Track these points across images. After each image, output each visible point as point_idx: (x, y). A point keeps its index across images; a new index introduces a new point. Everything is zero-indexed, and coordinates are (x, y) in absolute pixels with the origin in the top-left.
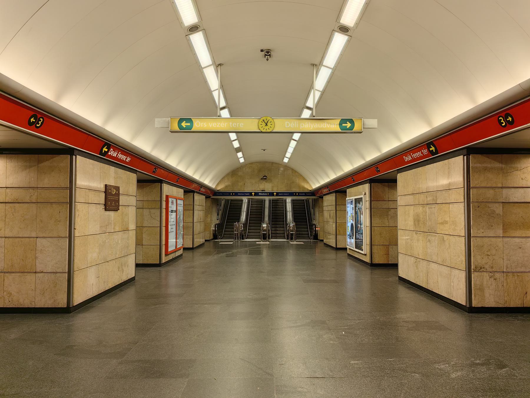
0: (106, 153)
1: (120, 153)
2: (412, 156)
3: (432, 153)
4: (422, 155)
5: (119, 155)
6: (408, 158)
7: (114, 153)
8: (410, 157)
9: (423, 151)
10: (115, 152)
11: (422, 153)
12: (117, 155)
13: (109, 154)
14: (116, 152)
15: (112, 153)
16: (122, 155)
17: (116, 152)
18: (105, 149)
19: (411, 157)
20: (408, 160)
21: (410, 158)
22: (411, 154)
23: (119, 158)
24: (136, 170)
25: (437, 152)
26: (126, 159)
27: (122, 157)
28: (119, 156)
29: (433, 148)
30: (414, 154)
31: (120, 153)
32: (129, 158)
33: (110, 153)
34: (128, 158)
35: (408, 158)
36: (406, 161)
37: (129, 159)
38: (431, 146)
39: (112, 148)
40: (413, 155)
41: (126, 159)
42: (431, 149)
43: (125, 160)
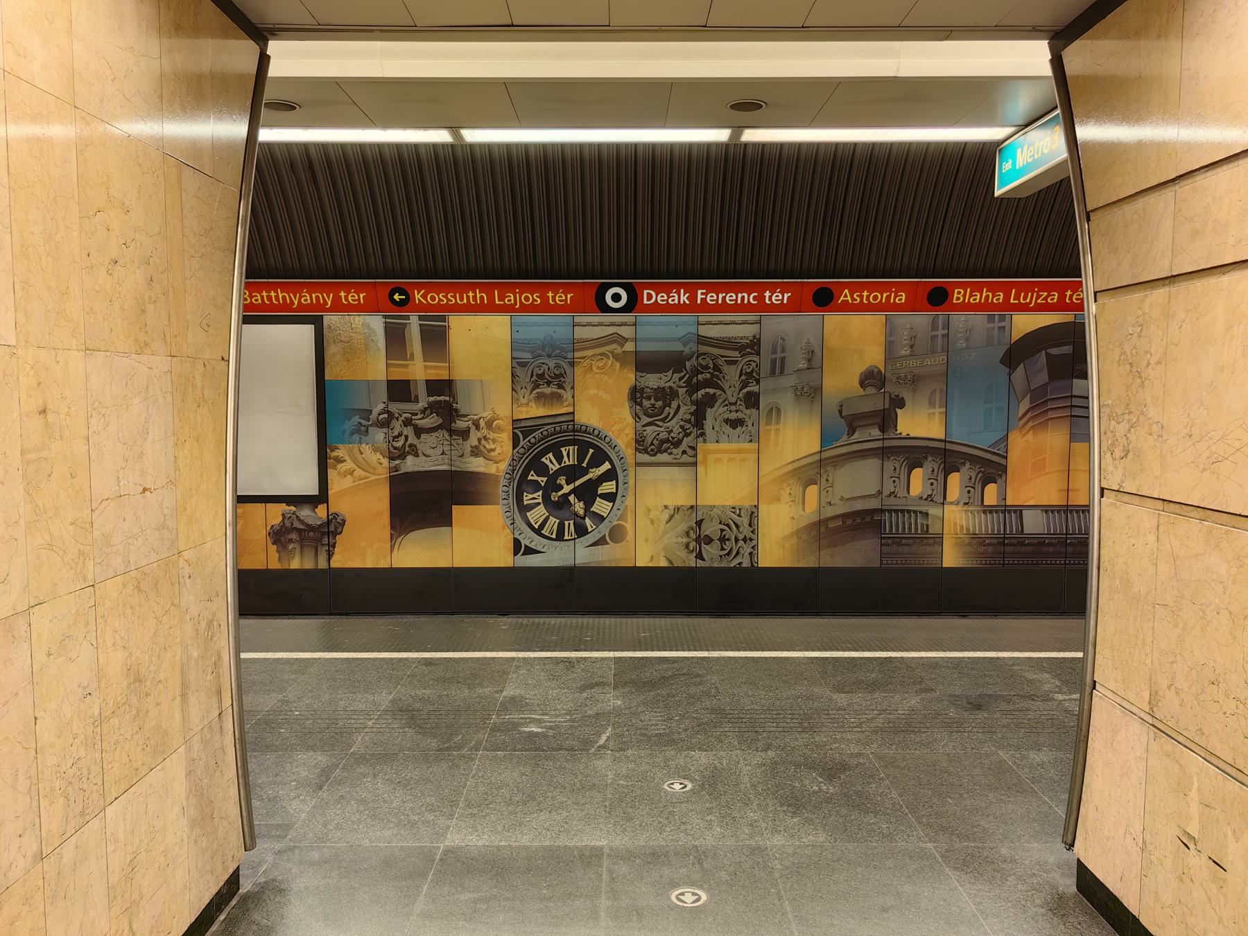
1: (699, 292)
5: (700, 297)
7: (669, 297)
12: (693, 298)
13: (645, 302)
16: (721, 296)
31: (699, 292)
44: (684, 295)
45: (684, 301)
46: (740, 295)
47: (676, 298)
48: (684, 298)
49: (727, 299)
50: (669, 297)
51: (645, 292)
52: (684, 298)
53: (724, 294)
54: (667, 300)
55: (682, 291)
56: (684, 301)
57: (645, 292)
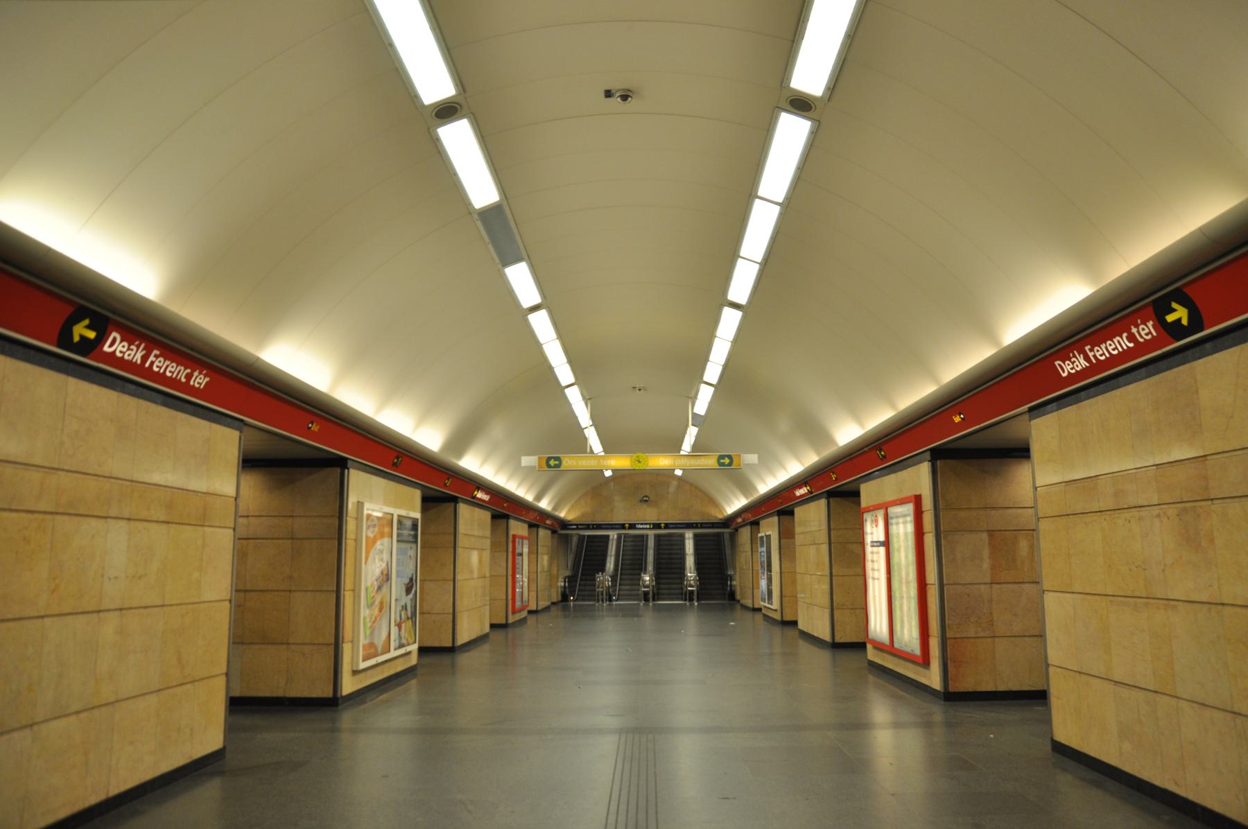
0: (87, 347)
2: (1091, 354)
3: (1176, 330)
4: (1131, 345)
5: (152, 358)
6: (1073, 363)
7: (129, 349)
8: (1082, 361)
9: (1134, 330)
10: (132, 347)
11: (1131, 338)
12: (145, 358)
13: (106, 348)
14: (138, 347)
15: (116, 346)
16: (167, 363)
17: (138, 347)
18: (82, 331)
19: (1087, 358)
20: (1073, 371)
21: (1080, 363)
22: (1087, 348)
23: (155, 369)
24: (242, 421)
25: (1196, 322)
26: (189, 377)
27: (172, 369)
28: (152, 363)
29: (1180, 314)
30: (1096, 348)
31: (156, 352)
32: (200, 373)
33: (111, 346)
34: (196, 374)
35: (1073, 363)
36: (1064, 375)
37: (200, 380)
38: (1174, 305)
39: (117, 331)
40: (1091, 350)
41: (189, 377)
42: (1170, 318)
43: (183, 380)
44: (142, 351)
45: (137, 360)
46: (179, 368)
47: (133, 353)
48: (138, 358)
49: (169, 369)
50: (129, 349)
51: (114, 334)
52: (138, 358)
53: (169, 362)
54: (124, 353)
55: (143, 346)
56: (137, 360)
57: (114, 334)
